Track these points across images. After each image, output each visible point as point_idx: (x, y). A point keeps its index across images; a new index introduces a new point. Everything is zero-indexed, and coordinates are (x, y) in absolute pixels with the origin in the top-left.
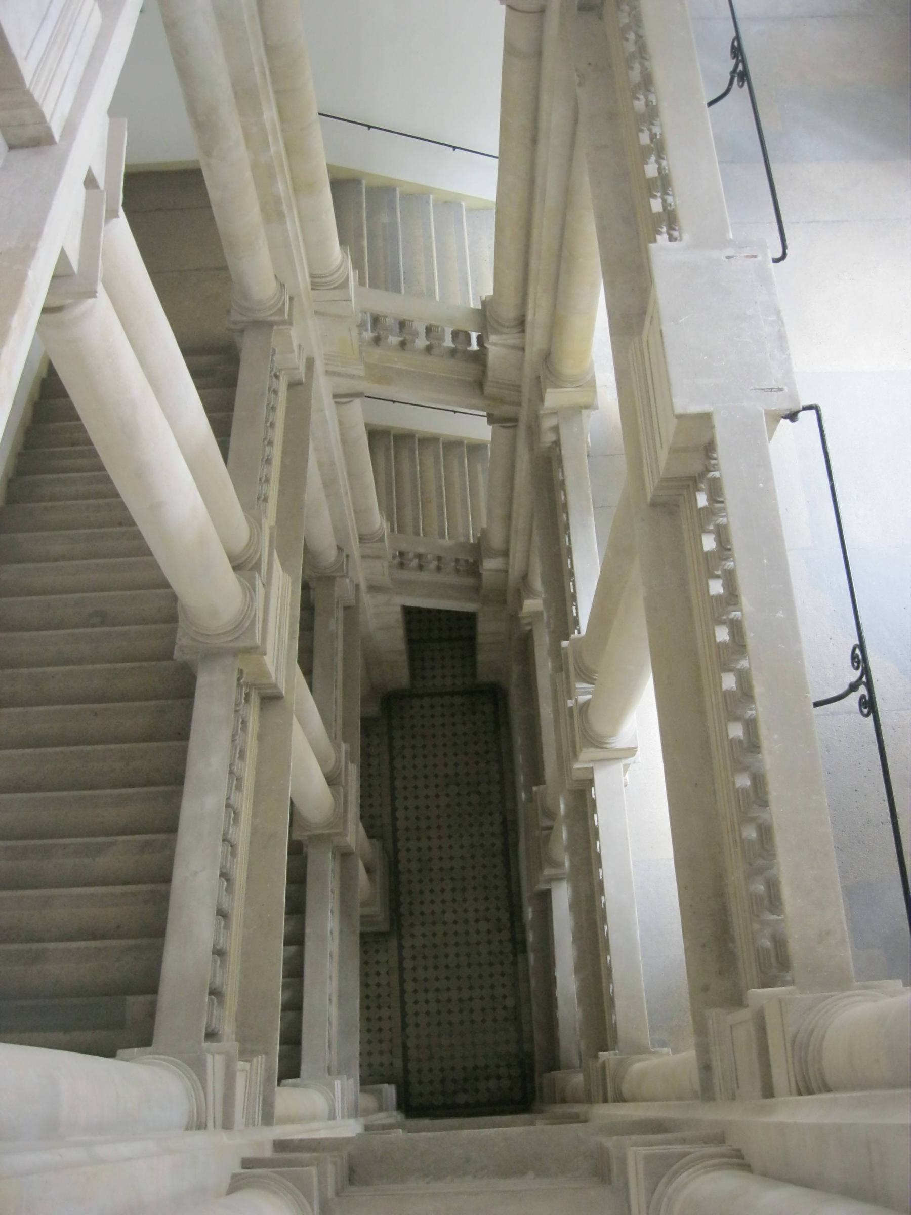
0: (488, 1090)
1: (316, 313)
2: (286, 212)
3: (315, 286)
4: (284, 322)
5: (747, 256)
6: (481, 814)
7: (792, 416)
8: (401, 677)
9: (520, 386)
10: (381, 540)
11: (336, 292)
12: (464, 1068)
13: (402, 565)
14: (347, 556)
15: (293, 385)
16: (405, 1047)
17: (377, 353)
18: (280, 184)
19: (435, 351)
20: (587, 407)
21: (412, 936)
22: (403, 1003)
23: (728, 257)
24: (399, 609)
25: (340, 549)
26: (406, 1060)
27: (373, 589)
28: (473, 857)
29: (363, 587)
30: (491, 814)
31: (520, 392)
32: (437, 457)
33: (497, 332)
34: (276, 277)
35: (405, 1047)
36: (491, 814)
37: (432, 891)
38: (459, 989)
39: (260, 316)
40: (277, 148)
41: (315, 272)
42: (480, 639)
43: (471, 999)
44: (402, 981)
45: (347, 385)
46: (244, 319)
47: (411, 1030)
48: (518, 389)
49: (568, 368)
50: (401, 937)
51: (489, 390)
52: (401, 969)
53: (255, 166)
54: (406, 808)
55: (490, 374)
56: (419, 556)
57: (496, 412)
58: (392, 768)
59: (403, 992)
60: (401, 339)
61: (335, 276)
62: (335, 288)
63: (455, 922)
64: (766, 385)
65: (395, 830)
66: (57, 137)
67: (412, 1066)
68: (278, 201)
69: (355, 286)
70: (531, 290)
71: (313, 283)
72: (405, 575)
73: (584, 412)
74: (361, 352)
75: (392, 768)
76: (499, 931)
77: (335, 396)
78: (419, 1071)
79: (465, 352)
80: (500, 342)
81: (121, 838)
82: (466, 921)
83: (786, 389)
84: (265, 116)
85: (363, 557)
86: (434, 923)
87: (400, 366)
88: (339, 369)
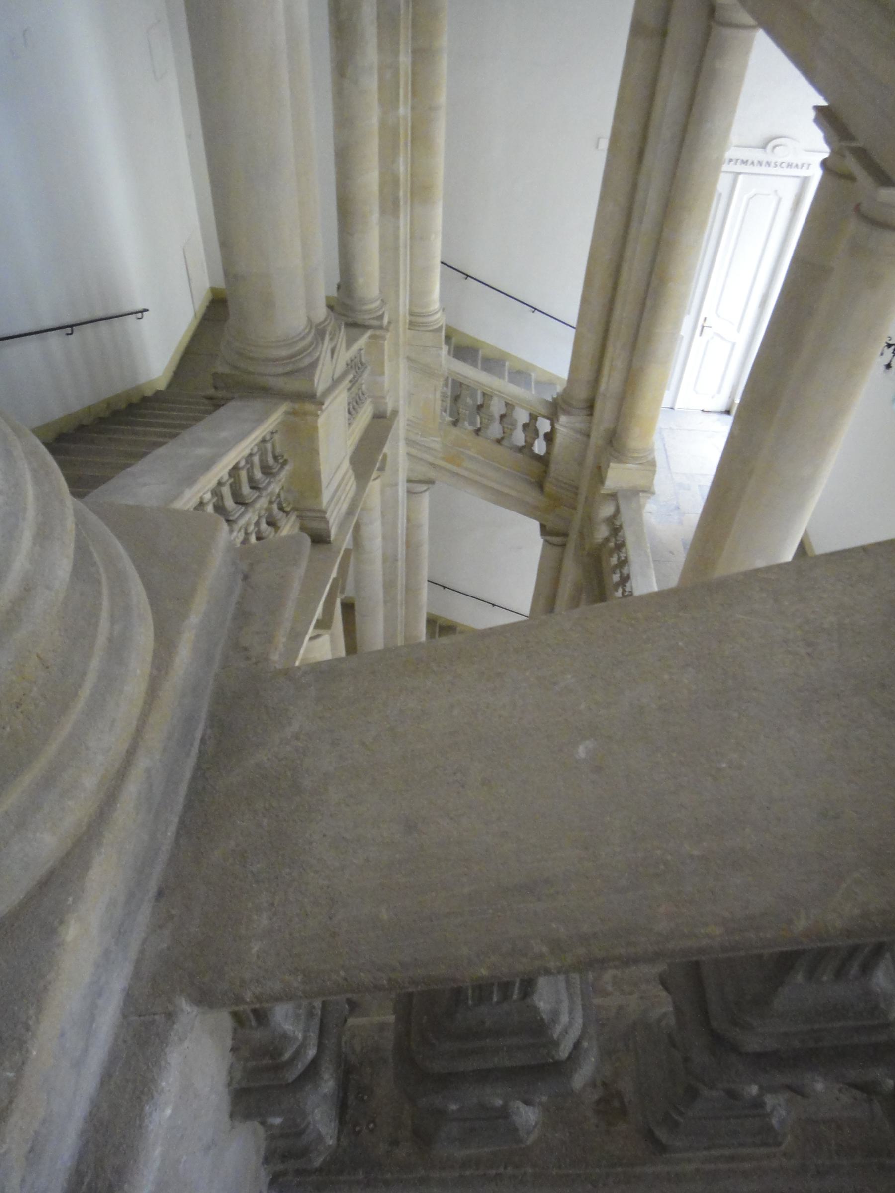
2: (402, 203)
3: (412, 325)
4: (381, 327)
9: (577, 488)
17: (455, 431)
18: (401, 159)
19: (505, 443)
20: (644, 491)
31: (576, 494)
33: (567, 413)
39: (360, 318)
41: (417, 310)
48: (575, 490)
49: (634, 443)
51: (549, 487)
53: (383, 125)
57: (549, 525)
62: (430, 331)
70: (610, 350)
71: (411, 323)
73: (641, 494)
88: (418, 438)
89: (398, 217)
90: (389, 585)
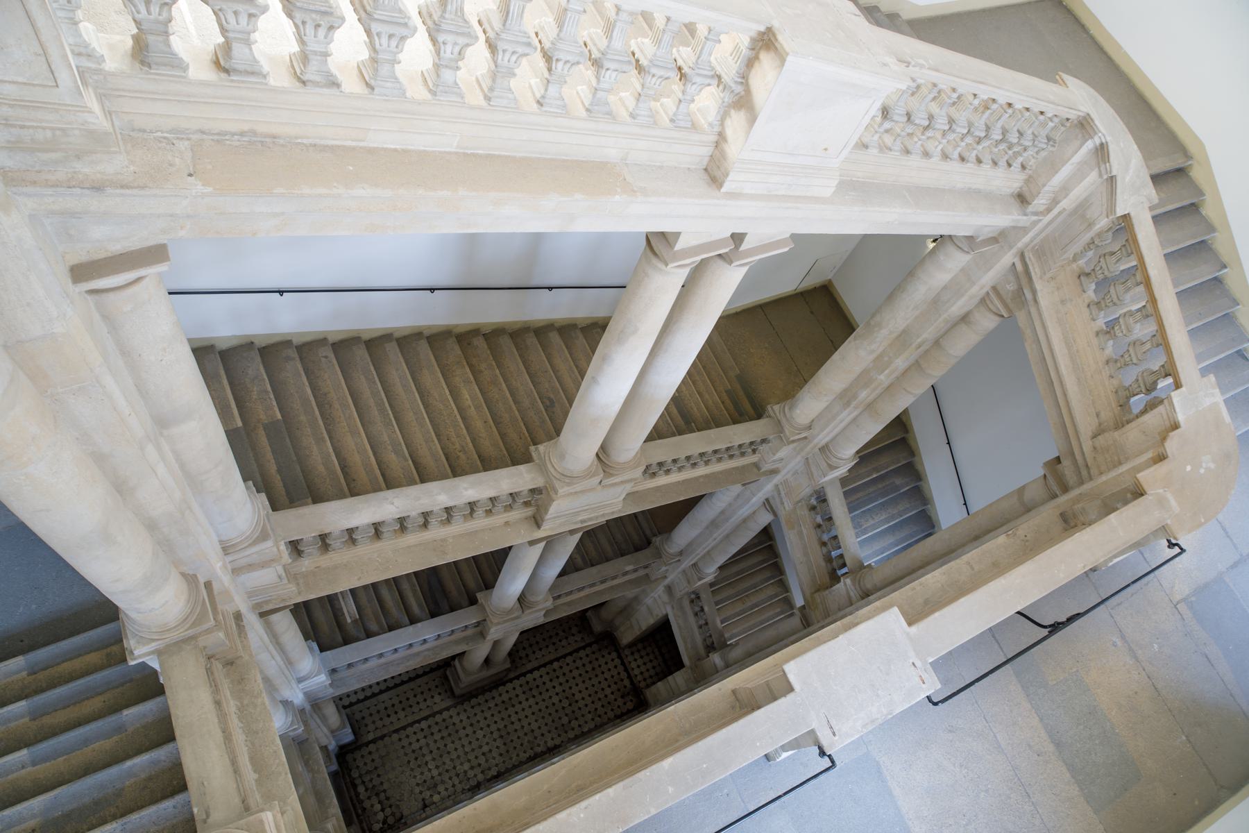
1: (807, 459)
5: (921, 676)
6: (556, 728)
7: (822, 753)
8: (626, 637)
10: (700, 579)
11: (826, 464)
13: (692, 601)
14: (679, 560)
15: (756, 466)
16: (382, 738)
17: (805, 512)
18: (865, 392)
21: (458, 714)
22: (411, 725)
23: (913, 664)
24: (664, 613)
25: (681, 553)
26: (373, 741)
27: (669, 589)
29: (667, 582)
30: (559, 736)
31: (826, 618)
32: (776, 595)
33: (853, 581)
34: (813, 421)
35: (382, 738)
36: (559, 736)
37: (493, 715)
40: (884, 378)
42: (670, 678)
44: (426, 718)
45: (776, 503)
46: (778, 414)
47: (395, 737)
50: (455, 706)
52: (433, 715)
53: (866, 372)
54: (541, 676)
55: (827, 592)
56: (702, 610)
58: (564, 656)
59: (419, 722)
60: (822, 523)
61: (834, 459)
63: (478, 739)
64: (833, 723)
65: (524, 675)
66: (723, 190)
67: (372, 747)
68: (855, 397)
69: (837, 477)
72: (686, 603)
74: (799, 501)
75: (564, 656)
76: (482, 772)
77: (767, 500)
78: (370, 753)
79: (834, 570)
80: (848, 587)
81: (410, 462)
82: (481, 747)
83: (837, 738)
84: (897, 361)
85: (684, 571)
86: (472, 725)
87: (805, 531)
89: (845, 409)
90: (714, 524)
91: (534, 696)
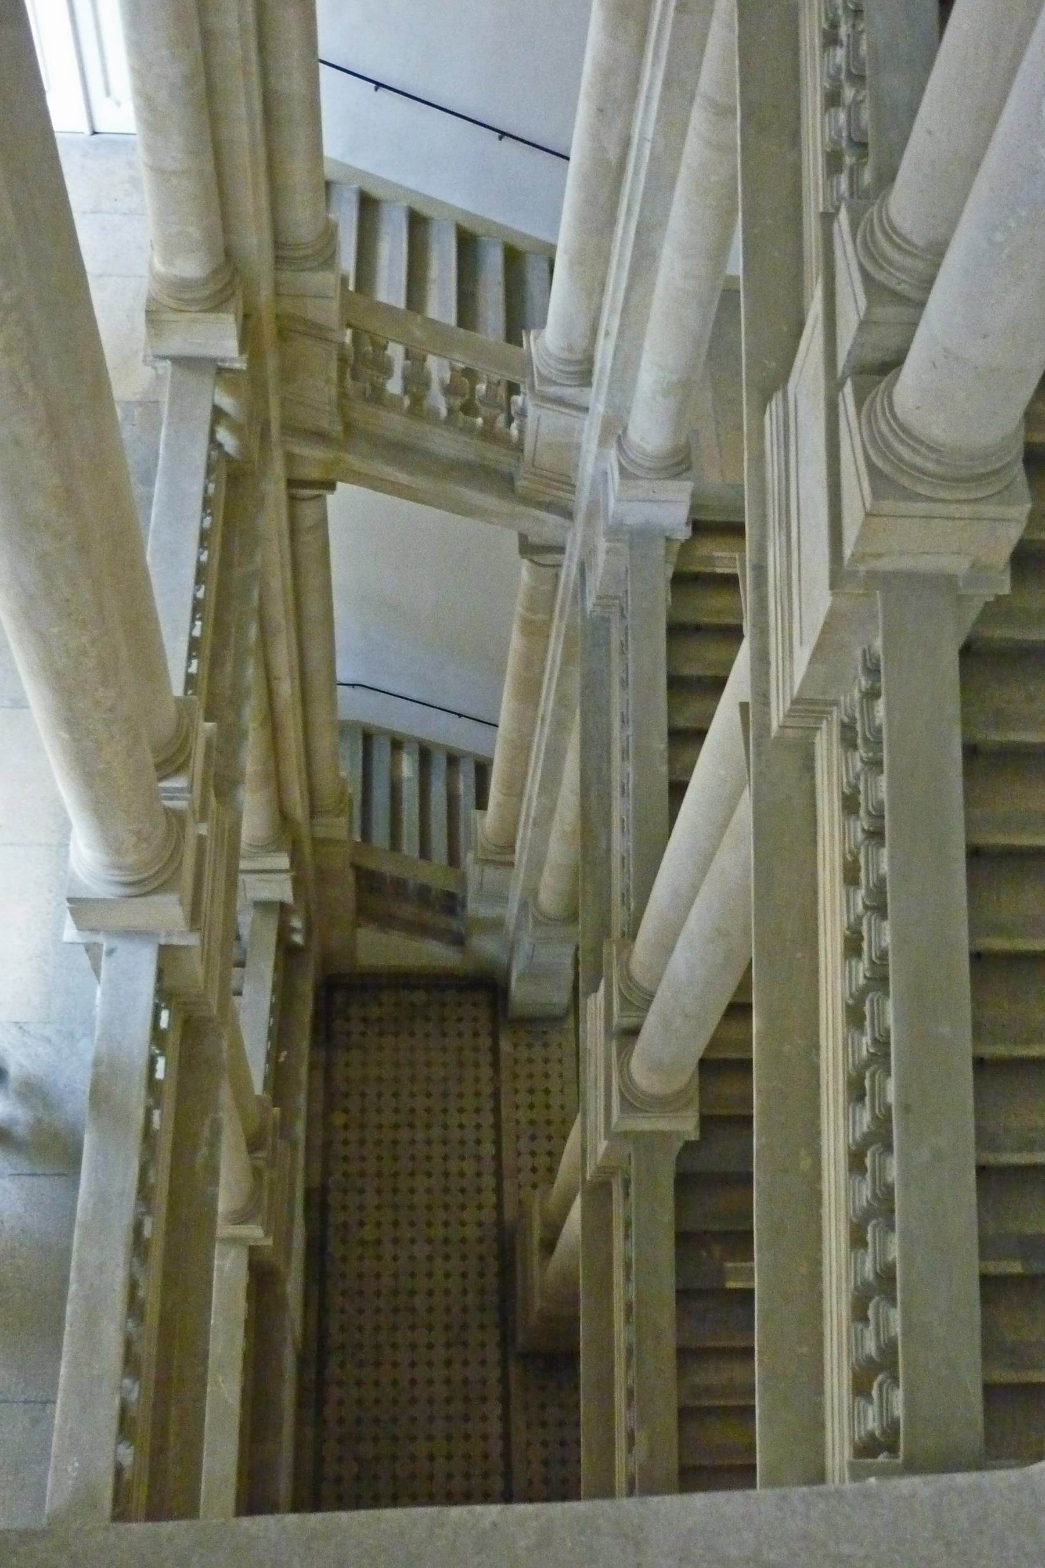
0: (380, 1005)
12: (412, 1034)
16: (496, 1065)
21: (480, 1224)
22: (497, 1127)
26: (495, 1050)
28: (378, 1346)
35: (496, 1065)
38: (413, 1142)
43: (396, 1127)
44: (498, 1157)
47: (487, 1089)
50: (499, 1222)
52: (498, 1174)
59: (497, 1143)
63: (413, 1241)
65: (505, 1400)
67: (485, 1041)
76: (345, 1225)
78: (476, 1034)
82: (396, 1241)
91: (448, 1400)
